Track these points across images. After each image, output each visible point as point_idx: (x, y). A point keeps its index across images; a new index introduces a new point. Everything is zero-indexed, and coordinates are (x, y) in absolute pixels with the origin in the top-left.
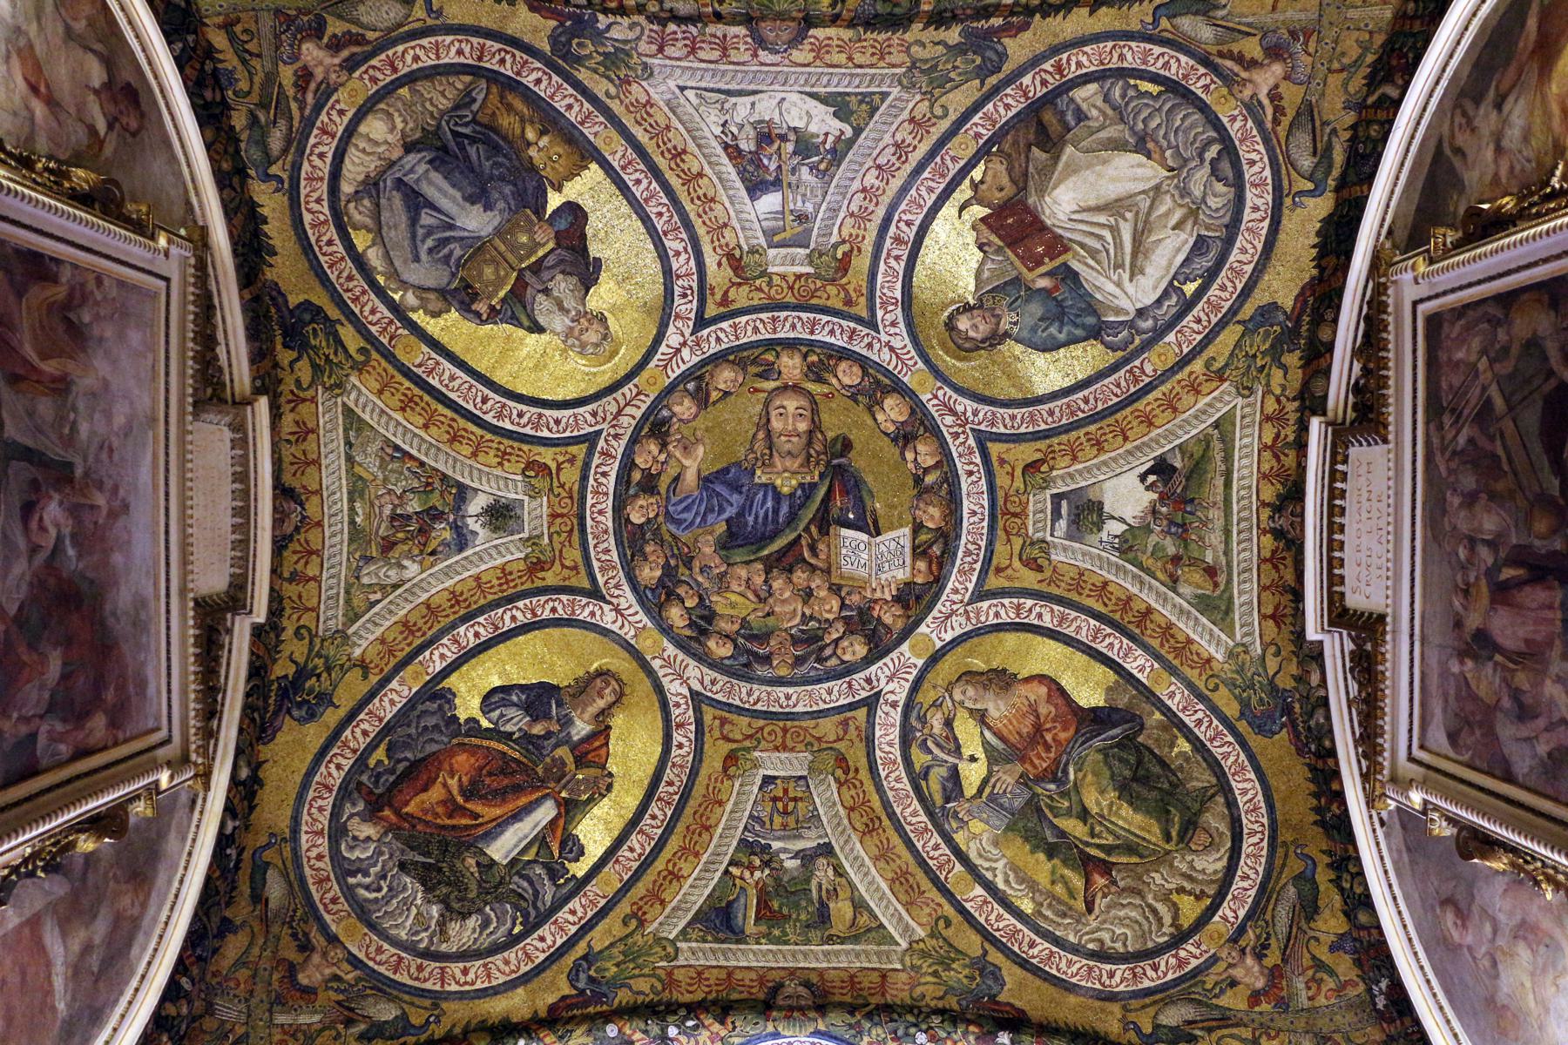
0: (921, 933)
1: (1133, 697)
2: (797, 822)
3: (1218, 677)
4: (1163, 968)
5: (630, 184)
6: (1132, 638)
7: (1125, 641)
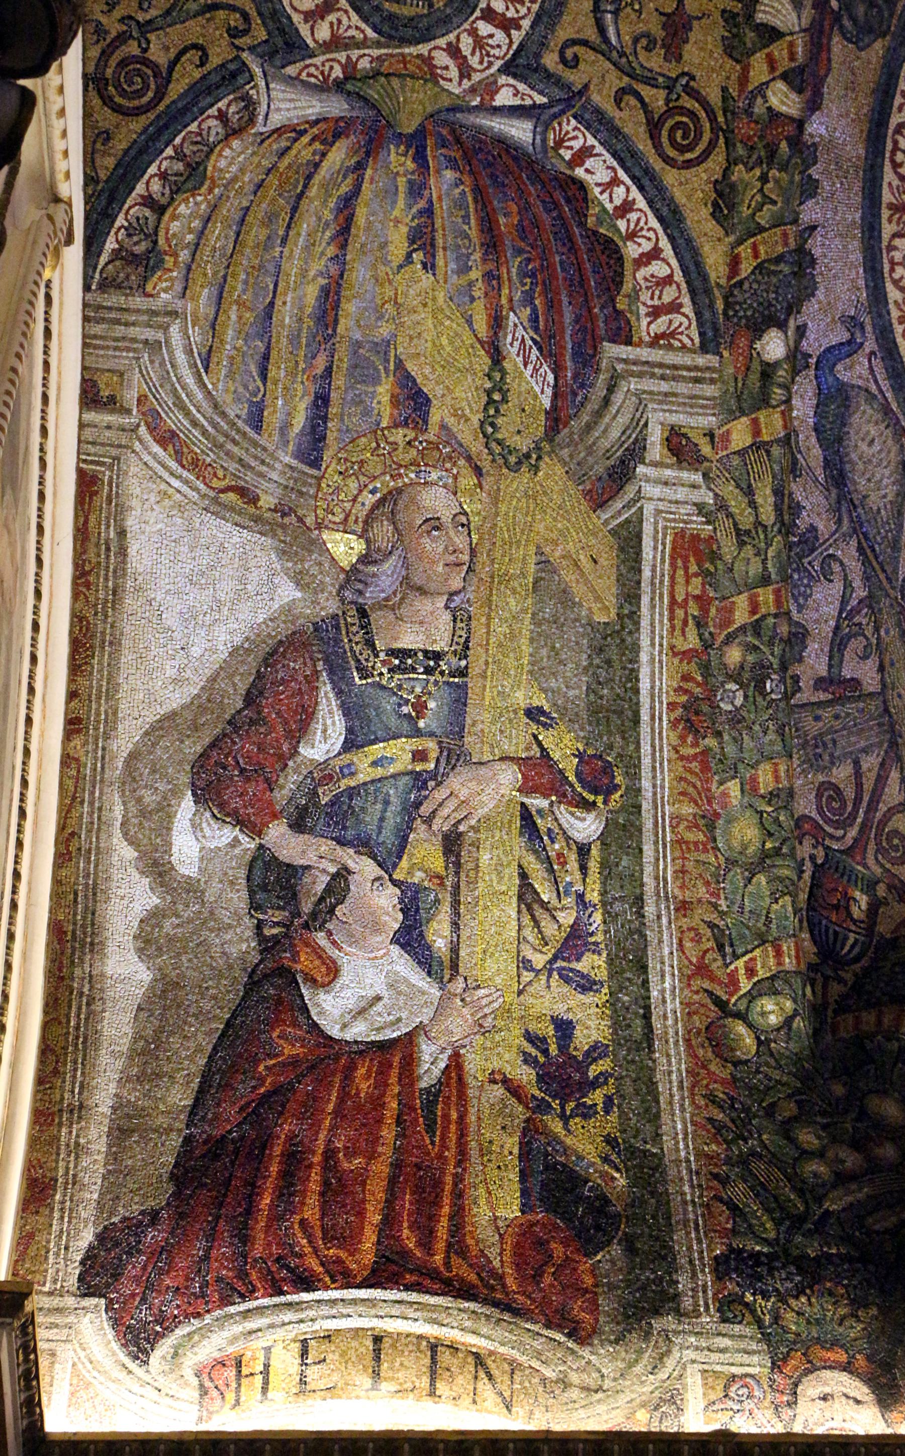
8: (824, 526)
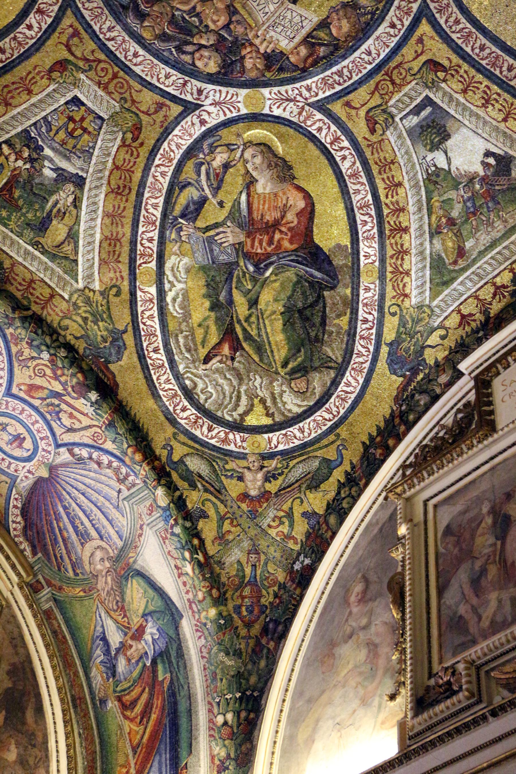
0: (97, 286)
1: (346, 266)
2: (74, 147)
3: (401, 310)
4: (214, 433)
6: (381, 232)
7: (375, 230)
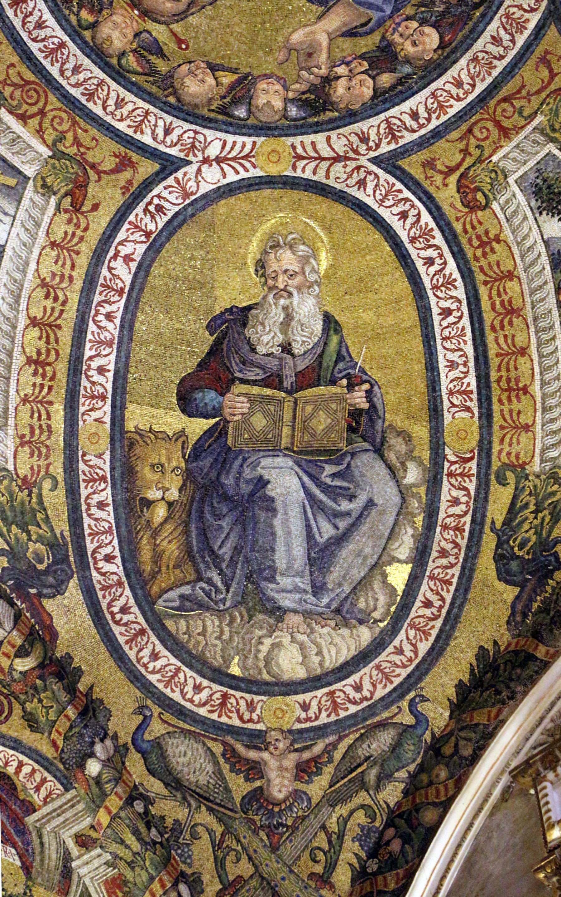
5: (110, 375)
8: (181, 814)
